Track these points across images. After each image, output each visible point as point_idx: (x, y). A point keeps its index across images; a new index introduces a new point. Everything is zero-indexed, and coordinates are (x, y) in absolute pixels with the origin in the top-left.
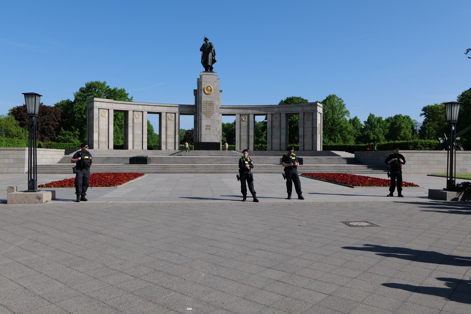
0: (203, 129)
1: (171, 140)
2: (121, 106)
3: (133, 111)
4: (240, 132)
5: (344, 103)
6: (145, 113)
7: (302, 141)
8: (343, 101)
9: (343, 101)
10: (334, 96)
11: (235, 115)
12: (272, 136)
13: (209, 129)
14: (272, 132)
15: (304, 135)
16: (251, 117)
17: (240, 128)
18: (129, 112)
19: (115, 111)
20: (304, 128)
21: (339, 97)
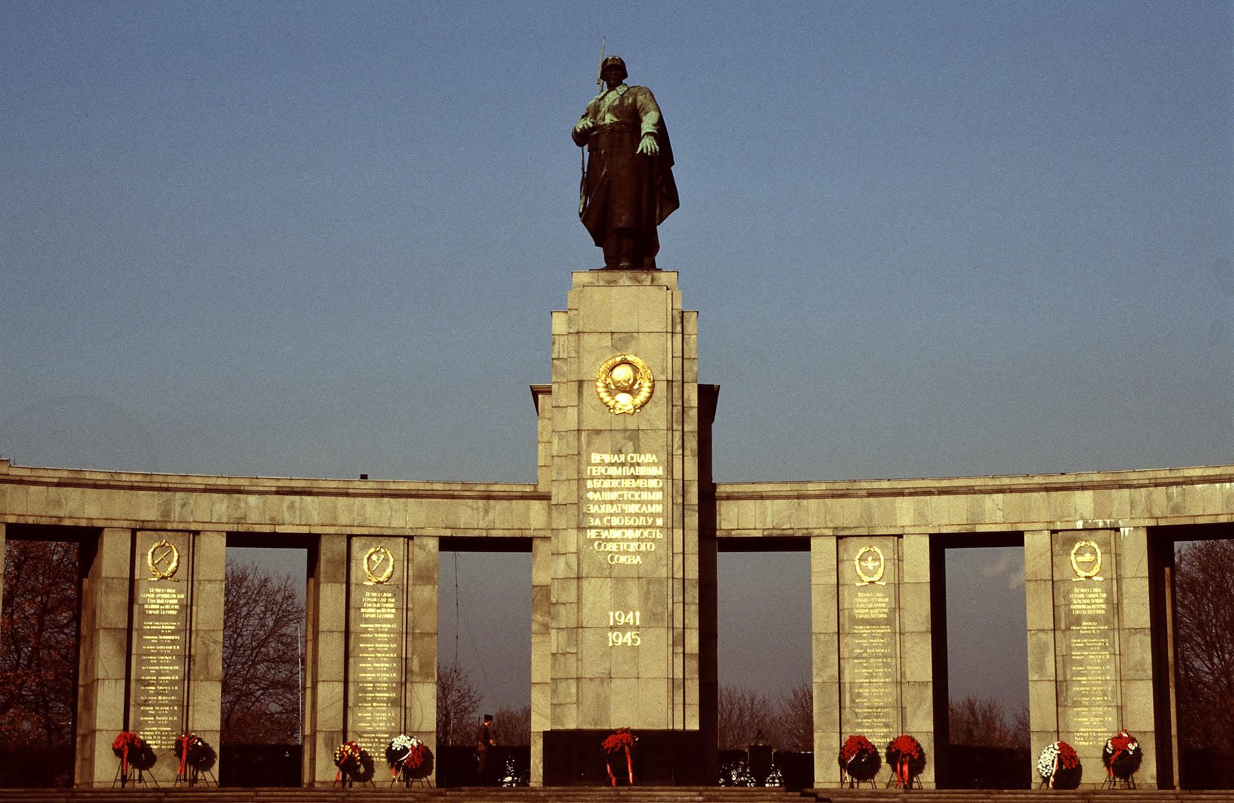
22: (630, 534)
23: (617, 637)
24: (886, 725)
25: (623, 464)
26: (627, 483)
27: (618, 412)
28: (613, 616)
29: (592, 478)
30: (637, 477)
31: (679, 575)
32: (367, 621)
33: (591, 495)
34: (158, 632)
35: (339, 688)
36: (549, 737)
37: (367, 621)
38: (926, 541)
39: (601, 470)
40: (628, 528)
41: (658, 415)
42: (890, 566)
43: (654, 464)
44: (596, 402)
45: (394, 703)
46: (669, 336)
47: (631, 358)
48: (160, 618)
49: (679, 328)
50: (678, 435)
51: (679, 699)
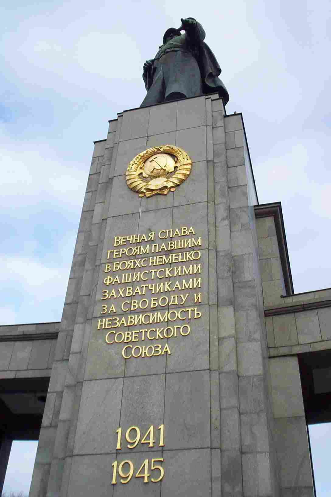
22: (158, 316)
23: (126, 466)
25: (152, 241)
26: (157, 260)
27: (149, 194)
28: (121, 436)
29: (111, 261)
30: (168, 253)
31: (231, 366)
40: (154, 310)
44: (126, 191)
46: (209, 129)
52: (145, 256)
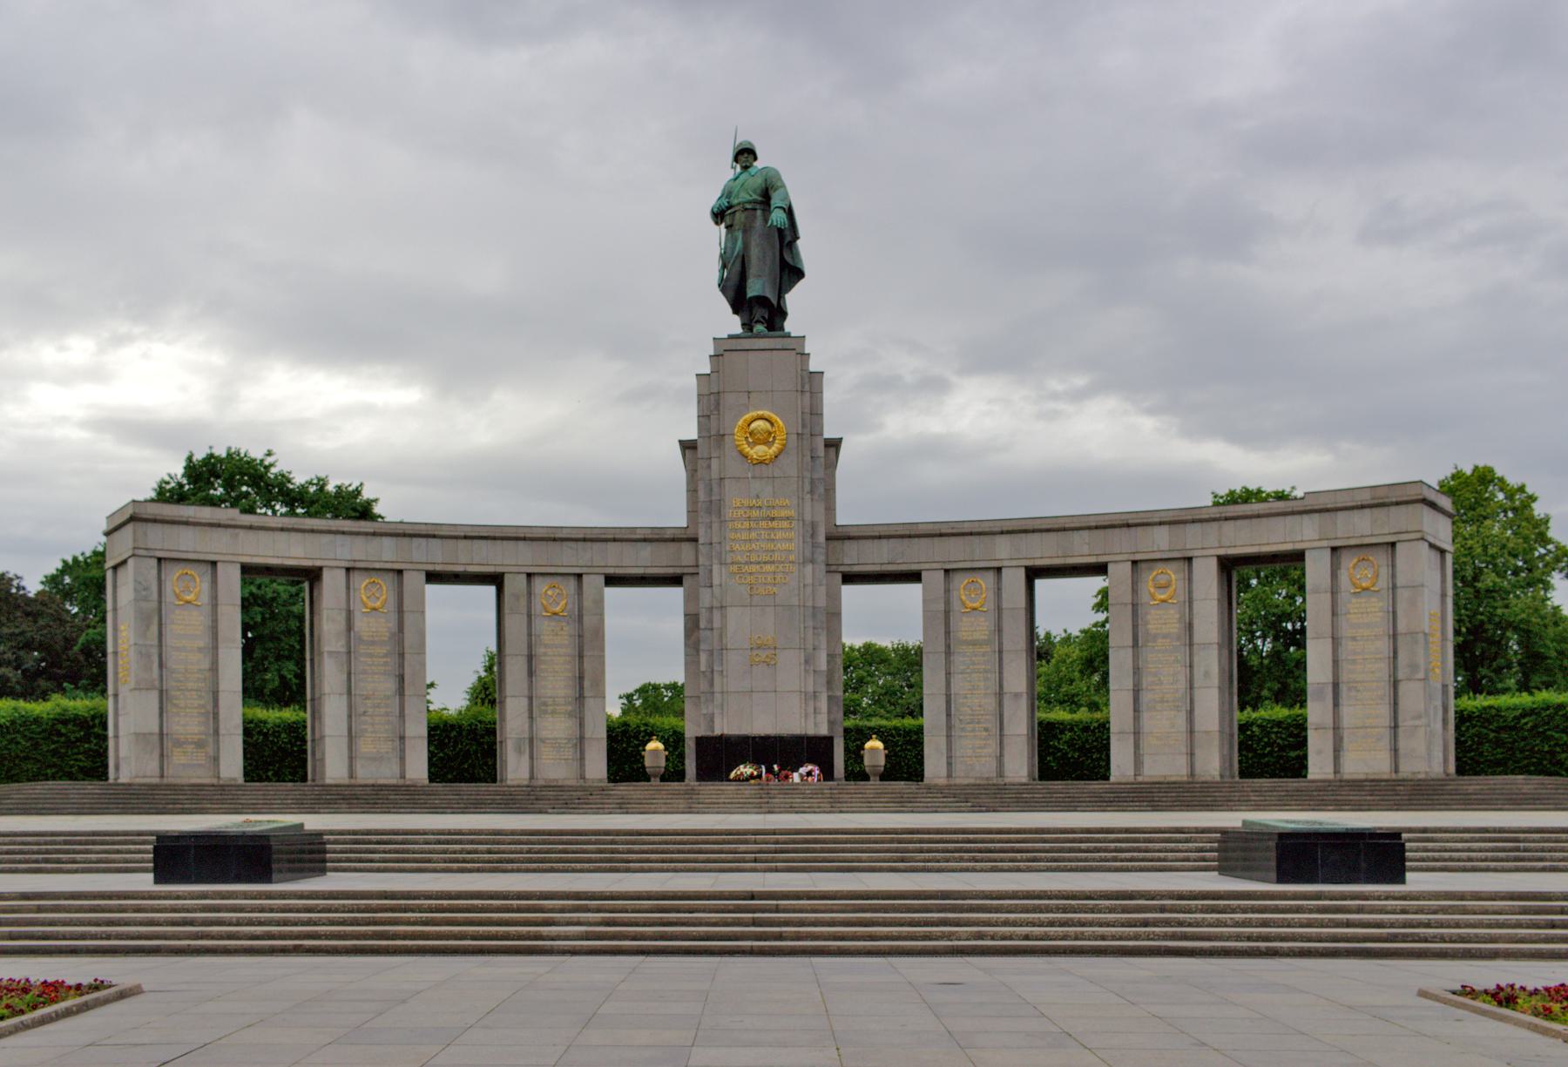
0: (734, 660)
1: (556, 727)
2: (282, 544)
3: (348, 569)
4: (948, 674)
5: (1538, 510)
6: (413, 580)
7: (1329, 721)
8: (1532, 499)
9: (1532, 499)
10: (1485, 477)
11: (914, 577)
12: (1137, 692)
13: (770, 664)
14: (1137, 671)
15: (1336, 686)
16: (1014, 580)
17: (948, 652)
18: (326, 575)
19: (247, 570)
20: (1336, 641)
21: (1513, 481)
24: (986, 730)
26: (763, 524)
31: (810, 604)
32: (546, 646)
33: (732, 536)
34: (371, 656)
35: (525, 702)
36: (700, 741)
37: (546, 646)
38: (1022, 572)
39: (741, 512)
41: (790, 465)
42: (991, 595)
43: (786, 507)
45: (570, 715)
47: (766, 413)
48: (373, 643)
49: (807, 387)
50: (807, 482)
51: (811, 710)
52: (757, 520)
